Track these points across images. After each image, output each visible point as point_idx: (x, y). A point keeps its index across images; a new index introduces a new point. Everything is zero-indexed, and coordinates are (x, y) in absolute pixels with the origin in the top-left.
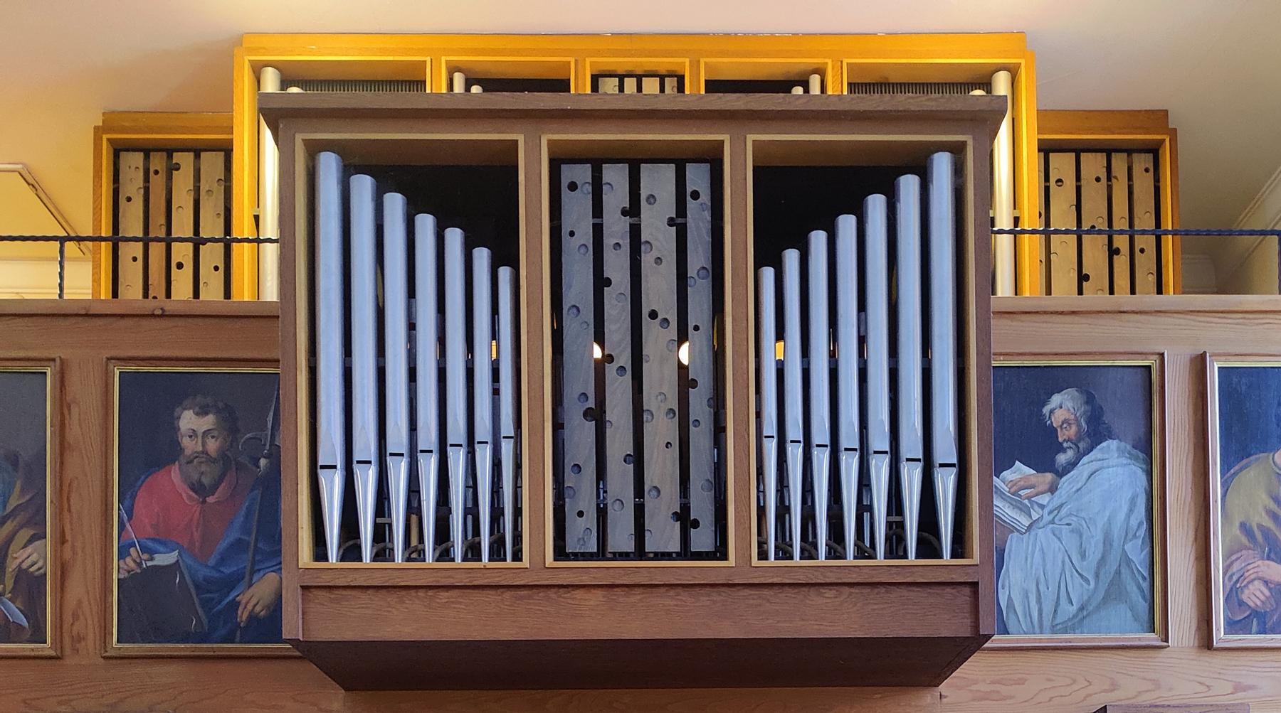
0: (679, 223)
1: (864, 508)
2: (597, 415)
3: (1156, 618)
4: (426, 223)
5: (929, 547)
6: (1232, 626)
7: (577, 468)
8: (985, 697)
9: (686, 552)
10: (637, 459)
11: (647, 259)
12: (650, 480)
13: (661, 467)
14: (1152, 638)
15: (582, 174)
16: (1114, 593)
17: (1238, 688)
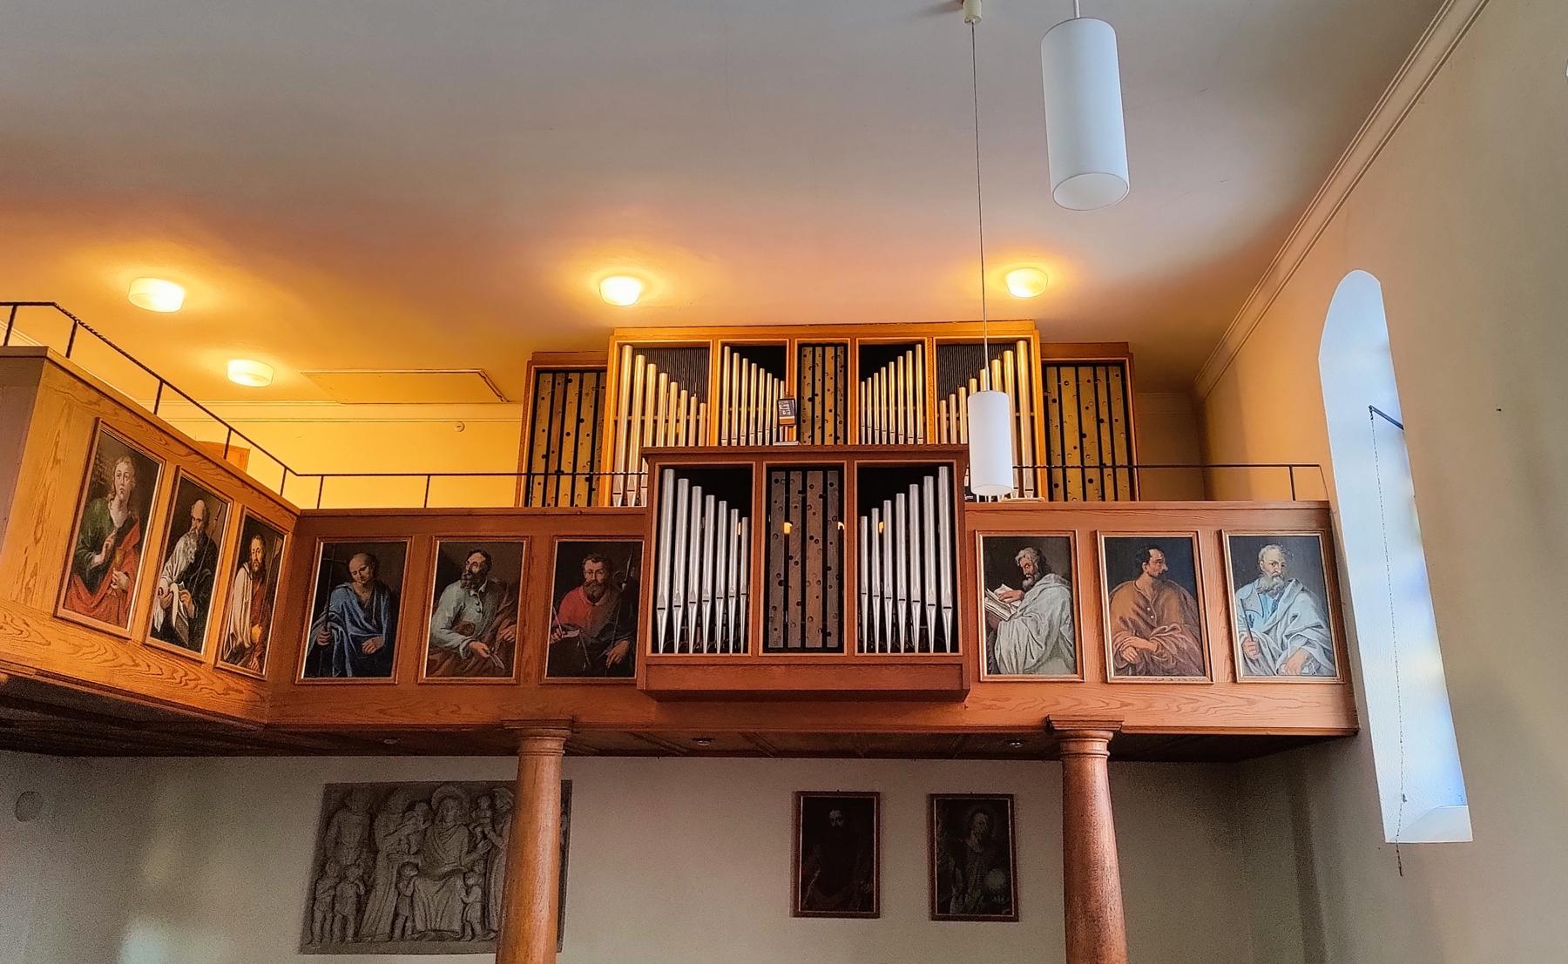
0: (824, 497)
1: (909, 624)
2: (785, 583)
3: (1076, 667)
4: (711, 499)
5: (940, 646)
6: (1117, 671)
7: (775, 608)
8: (990, 707)
9: (825, 649)
10: (803, 604)
11: (810, 513)
12: (809, 613)
13: (813, 607)
14: (1076, 678)
15: (782, 475)
16: (1055, 653)
17: (1124, 705)
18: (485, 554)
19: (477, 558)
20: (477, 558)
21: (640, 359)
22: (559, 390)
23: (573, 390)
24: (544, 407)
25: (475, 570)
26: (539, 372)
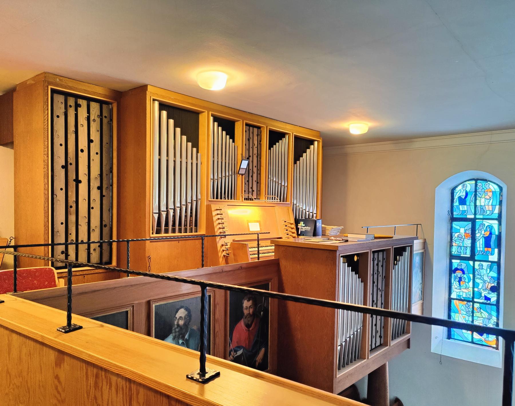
18: (187, 309)
19: (182, 313)
20: (182, 313)
21: (164, 113)
22: (71, 113)
23: (83, 112)
24: (60, 123)
25: (181, 322)
26: (53, 91)
